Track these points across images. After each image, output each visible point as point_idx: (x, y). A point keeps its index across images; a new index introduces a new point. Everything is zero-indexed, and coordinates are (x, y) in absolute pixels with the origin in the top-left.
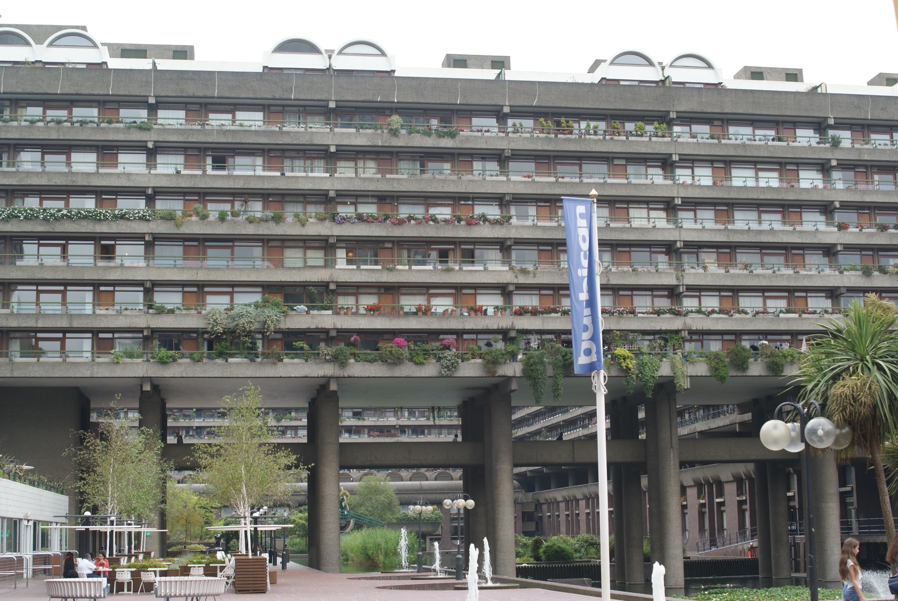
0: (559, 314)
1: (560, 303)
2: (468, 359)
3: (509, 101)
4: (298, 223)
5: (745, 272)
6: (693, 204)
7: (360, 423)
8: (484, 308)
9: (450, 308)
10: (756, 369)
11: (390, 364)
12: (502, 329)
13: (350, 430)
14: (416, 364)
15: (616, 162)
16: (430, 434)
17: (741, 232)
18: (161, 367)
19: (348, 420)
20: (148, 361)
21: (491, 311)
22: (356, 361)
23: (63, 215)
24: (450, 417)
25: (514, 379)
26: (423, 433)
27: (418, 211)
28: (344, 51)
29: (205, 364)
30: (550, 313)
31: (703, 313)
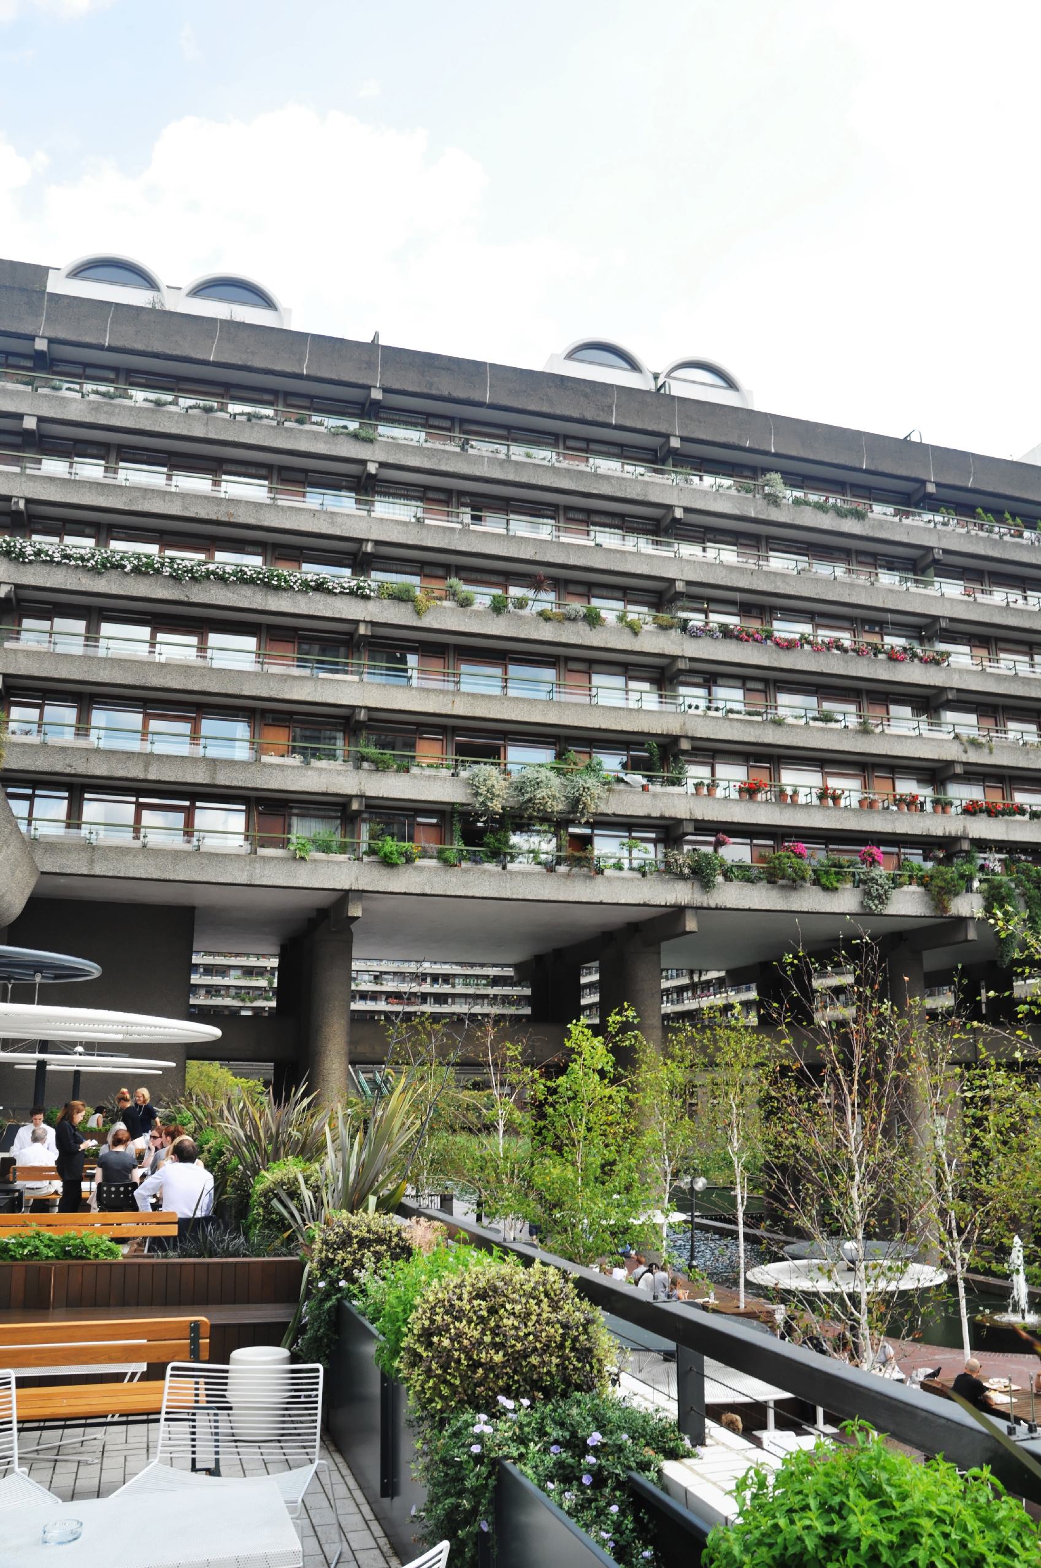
1: (1012, 798)
2: (901, 885)
3: (935, 475)
4: (627, 630)
7: (378, 988)
11: (783, 887)
13: (364, 996)
14: (826, 889)
16: (453, 1003)
18: (385, 872)
19: (365, 984)
20: (359, 859)
21: (929, 807)
23: (209, 573)
24: (477, 985)
26: (446, 1002)
29: (467, 871)
30: (1011, 814)
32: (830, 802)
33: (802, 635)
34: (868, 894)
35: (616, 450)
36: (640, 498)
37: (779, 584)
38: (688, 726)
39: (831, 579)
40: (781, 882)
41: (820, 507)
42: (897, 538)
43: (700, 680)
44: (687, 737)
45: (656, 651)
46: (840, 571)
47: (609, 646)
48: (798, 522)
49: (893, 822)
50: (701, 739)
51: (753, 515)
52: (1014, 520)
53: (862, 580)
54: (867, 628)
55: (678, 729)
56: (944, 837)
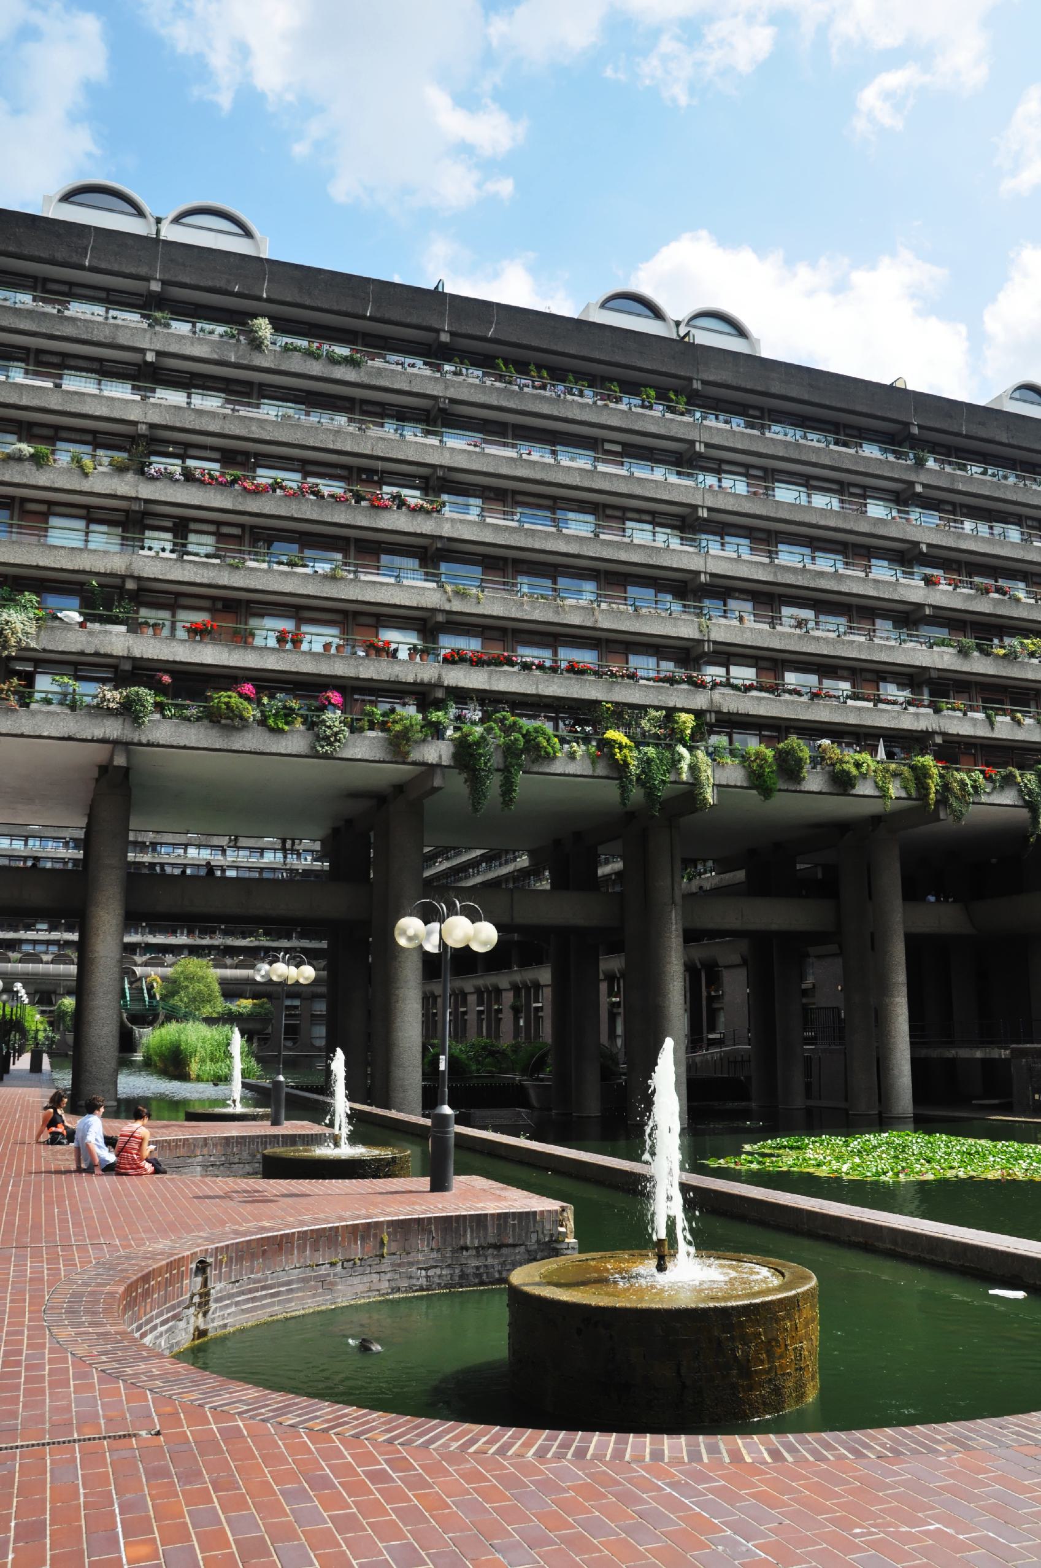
0: (516, 669)
2: (361, 730)
3: (450, 325)
5: (798, 631)
6: (722, 525)
8: (393, 646)
9: (336, 641)
10: (814, 781)
11: (225, 726)
12: (422, 684)
15: (608, 446)
17: (794, 570)
21: (403, 654)
22: (164, 717)
25: (439, 771)
27: (292, 479)
28: (183, 221)
30: (501, 664)
31: (735, 687)
32: (289, 646)
33: (275, 479)
34: (318, 738)
35: (103, 295)
36: (109, 340)
37: (253, 428)
38: (134, 566)
39: (334, 430)
40: (223, 721)
41: (309, 354)
42: (396, 386)
43: (169, 524)
44: (132, 577)
45: (107, 492)
46: (341, 420)
47: (56, 486)
48: (283, 368)
49: (357, 667)
50: (149, 579)
51: (233, 359)
52: (539, 372)
53: (433, 441)
54: (364, 477)
55: (124, 567)
56: (414, 684)
